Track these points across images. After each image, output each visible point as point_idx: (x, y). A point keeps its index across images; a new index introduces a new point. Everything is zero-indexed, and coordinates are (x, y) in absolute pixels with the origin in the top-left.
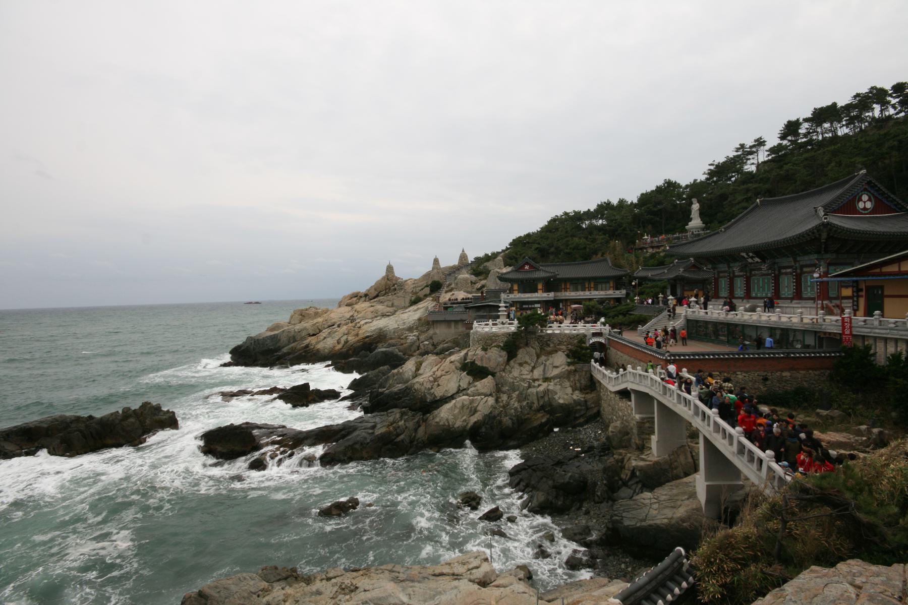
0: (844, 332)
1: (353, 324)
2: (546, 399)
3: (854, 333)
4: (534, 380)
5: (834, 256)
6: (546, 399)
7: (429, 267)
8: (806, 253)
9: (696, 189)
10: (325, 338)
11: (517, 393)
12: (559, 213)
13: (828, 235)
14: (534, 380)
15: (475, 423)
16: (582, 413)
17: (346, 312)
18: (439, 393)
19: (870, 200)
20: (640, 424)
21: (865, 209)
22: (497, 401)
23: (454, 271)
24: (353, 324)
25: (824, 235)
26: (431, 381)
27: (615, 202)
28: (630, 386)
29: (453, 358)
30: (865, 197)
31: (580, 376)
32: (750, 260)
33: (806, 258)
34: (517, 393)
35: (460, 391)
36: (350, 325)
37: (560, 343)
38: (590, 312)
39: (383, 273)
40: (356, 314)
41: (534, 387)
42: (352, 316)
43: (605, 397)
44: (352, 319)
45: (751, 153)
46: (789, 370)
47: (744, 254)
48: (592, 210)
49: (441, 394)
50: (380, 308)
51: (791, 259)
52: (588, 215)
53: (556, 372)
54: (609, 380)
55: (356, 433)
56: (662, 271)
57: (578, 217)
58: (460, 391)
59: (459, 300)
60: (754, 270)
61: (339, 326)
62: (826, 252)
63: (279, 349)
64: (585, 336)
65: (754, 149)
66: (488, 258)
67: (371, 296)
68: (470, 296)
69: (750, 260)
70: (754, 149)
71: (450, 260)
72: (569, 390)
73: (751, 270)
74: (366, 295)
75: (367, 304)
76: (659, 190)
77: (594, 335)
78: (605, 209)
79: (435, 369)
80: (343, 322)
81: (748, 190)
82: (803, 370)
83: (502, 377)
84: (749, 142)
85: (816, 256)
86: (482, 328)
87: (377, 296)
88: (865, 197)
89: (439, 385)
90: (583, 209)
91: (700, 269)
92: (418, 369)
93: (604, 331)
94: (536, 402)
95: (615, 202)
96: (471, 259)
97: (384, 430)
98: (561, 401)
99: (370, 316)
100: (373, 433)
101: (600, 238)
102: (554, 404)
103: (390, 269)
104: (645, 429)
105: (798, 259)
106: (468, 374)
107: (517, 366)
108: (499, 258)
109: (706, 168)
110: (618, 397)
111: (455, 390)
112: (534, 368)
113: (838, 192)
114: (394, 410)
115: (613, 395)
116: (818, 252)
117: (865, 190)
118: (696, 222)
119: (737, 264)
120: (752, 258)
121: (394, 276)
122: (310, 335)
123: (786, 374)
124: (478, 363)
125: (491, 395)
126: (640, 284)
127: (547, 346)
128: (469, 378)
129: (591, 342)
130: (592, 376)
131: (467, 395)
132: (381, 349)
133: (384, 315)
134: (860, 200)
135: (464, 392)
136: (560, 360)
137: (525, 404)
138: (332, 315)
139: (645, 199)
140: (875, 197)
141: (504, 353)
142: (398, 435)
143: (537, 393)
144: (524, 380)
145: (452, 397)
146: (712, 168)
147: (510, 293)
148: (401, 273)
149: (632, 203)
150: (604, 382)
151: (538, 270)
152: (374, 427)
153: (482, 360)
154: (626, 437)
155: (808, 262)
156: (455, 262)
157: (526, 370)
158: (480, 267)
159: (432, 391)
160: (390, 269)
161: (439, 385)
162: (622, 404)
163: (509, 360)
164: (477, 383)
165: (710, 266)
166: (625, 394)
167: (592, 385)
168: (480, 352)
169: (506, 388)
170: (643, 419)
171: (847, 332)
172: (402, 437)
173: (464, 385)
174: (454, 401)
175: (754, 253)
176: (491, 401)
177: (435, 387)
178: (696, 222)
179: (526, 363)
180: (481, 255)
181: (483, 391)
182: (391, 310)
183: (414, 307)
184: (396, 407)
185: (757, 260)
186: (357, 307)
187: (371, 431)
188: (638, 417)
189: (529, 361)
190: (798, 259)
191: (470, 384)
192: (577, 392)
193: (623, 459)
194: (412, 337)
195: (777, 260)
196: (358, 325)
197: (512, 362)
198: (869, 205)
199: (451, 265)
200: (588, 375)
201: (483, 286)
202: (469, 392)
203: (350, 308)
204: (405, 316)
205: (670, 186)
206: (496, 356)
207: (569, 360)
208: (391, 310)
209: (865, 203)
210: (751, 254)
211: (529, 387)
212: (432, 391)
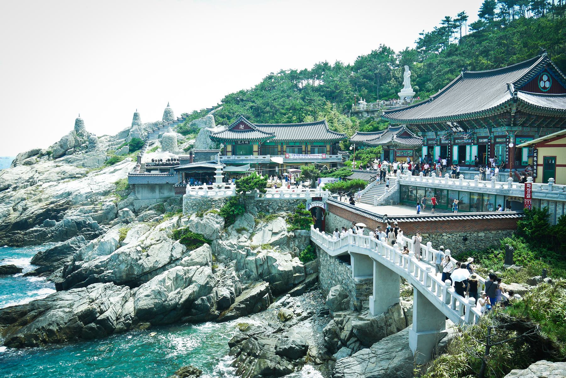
0: (526, 196)
1: (34, 187)
2: (266, 267)
3: (533, 197)
4: (254, 248)
5: (521, 128)
6: (266, 267)
7: (127, 124)
8: (499, 125)
9: (408, 57)
11: (235, 261)
12: (276, 71)
13: (517, 109)
14: (254, 248)
15: (190, 295)
16: (302, 279)
18: (148, 263)
19: (548, 80)
20: (359, 286)
21: (545, 88)
22: (214, 271)
23: (156, 128)
25: (514, 110)
26: (138, 252)
27: (332, 64)
28: (350, 250)
29: (163, 225)
30: (545, 78)
31: (299, 242)
32: (454, 129)
33: (499, 129)
34: (235, 261)
35: (173, 261)
37: (280, 209)
38: (311, 176)
40: (37, 175)
41: (253, 254)
42: (32, 178)
43: (323, 263)
45: (455, 27)
46: (484, 230)
47: (450, 124)
48: (309, 69)
49: (151, 265)
50: (69, 169)
51: (487, 130)
52: (305, 74)
54: (329, 243)
56: (377, 136)
57: (294, 76)
58: (173, 261)
59: (164, 161)
60: (458, 139)
61: (15, 189)
62: (515, 125)
64: (305, 201)
65: (458, 23)
66: (196, 115)
68: (177, 157)
69: (454, 129)
70: (458, 23)
71: (152, 116)
73: (455, 139)
74: (48, 153)
75: (51, 163)
76: (375, 55)
77: (314, 199)
78: (321, 70)
79: (143, 238)
81: (452, 62)
82: (494, 230)
83: (219, 245)
84: (454, 16)
85: (507, 128)
86: (195, 192)
87: (64, 154)
88: (545, 78)
89: (148, 256)
90: (299, 68)
91: (410, 137)
92: (122, 239)
93: (323, 196)
94: (254, 270)
95: (332, 64)
96: (177, 115)
99: (56, 177)
101: (317, 98)
102: (274, 272)
104: (364, 290)
105: (493, 130)
106: (181, 243)
107: (234, 233)
108: (210, 115)
109: (417, 37)
110: (337, 262)
111: (168, 260)
112: (252, 235)
113: (526, 71)
114: (95, 285)
115: (332, 260)
116: (509, 125)
117: (546, 71)
118: (407, 91)
119: (443, 132)
120: (456, 127)
123: (482, 234)
125: (207, 264)
126: (357, 149)
127: (267, 210)
129: (311, 207)
130: (311, 243)
131: (181, 265)
132: (72, 215)
133: (73, 177)
134: (541, 79)
135: (177, 263)
136: (280, 225)
137: (243, 272)
139: (361, 63)
140: (552, 78)
142: (102, 312)
143: (256, 260)
144: (242, 247)
145: (164, 268)
146: (422, 37)
147: (223, 155)
148: (92, 128)
149: (349, 66)
150: (324, 246)
151: (253, 130)
152: (71, 306)
153: (197, 227)
154: (345, 300)
155: (500, 134)
156: (159, 117)
157: (244, 237)
158: (188, 125)
159: (140, 262)
161: (148, 256)
162: (342, 268)
163: (226, 227)
164: (191, 252)
165: (420, 134)
166: (344, 258)
167: (311, 252)
168: (194, 218)
169: (222, 257)
170: (361, 281)
171: (528, 197)
173: (177, 254)
174: (166, 272)
175: (459, 122)
176: (208, 270)
177: (143, 257)
178: (407, 91)
179: (244, 229)
180: (190, 112)
181: (197, 260)
182: (83, 170)
183: (111, 168)
185: (460, 129)
187: (67, 310)
188: (357, 280)
189: (248, 228)
190: (493, 130)
191: (183, 253)
192: (297, 259)
193: (342, 321)
194: (110, 201)
195: (476, 131)
198: (548, 85)
199: (154, 121)
200: (307, 241)
201: (192, 146)
202: (183, 262)
203: (28, 168)
204: (99, 178)
205: (384, 53)
206: (213, 221)
207: (289, 226)
208: (83, 170)
209: (545, 83)
210: (455, 124)
211: (248, 255)
212: (140, 262)
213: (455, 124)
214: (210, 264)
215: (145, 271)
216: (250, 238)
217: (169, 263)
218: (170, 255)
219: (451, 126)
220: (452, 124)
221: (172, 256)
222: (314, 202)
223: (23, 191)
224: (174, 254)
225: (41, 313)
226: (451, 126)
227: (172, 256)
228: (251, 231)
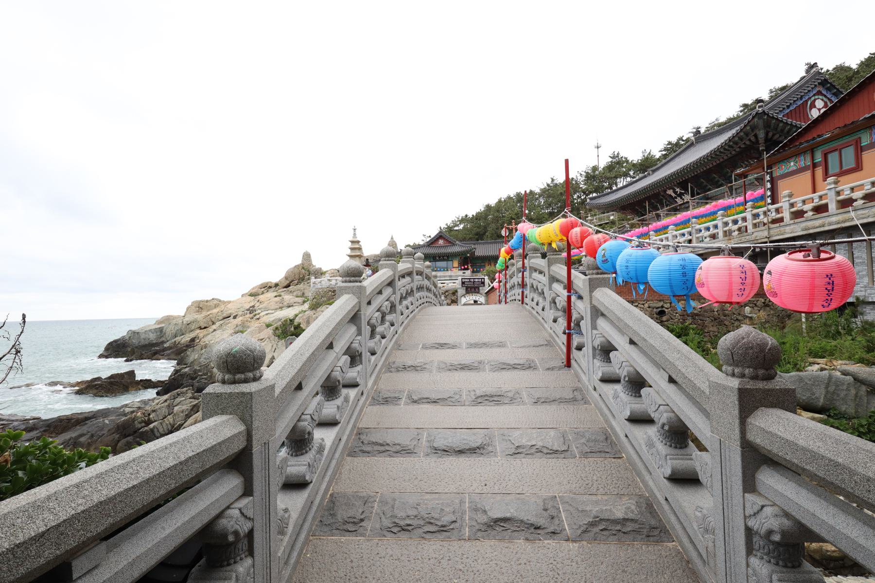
1: (252, 315)
10: (215, 330)
12: (504, 196)
17: (249, 302)
24: (252, 315)
36: (248, 315)
39: (298, 261)
40: (258, 304)
42: (253, 306)
44: (252, 310)
50: (288, 298)
61: (235, 317)
63: (163, 342)
67: (281, 285)
80: (240, 313)
103: (307, 256)
121: (311, 264)
122: (201, 328)
138: (229, 306)
148: (318, 262)
160: (307, 256)
182: (300, 300)
186: (261, 297)
196: (258, 316)
213: (678, 190)
219: (673, 195)
220: (675, 192)
223: (241, 318)
226: (673, 195)
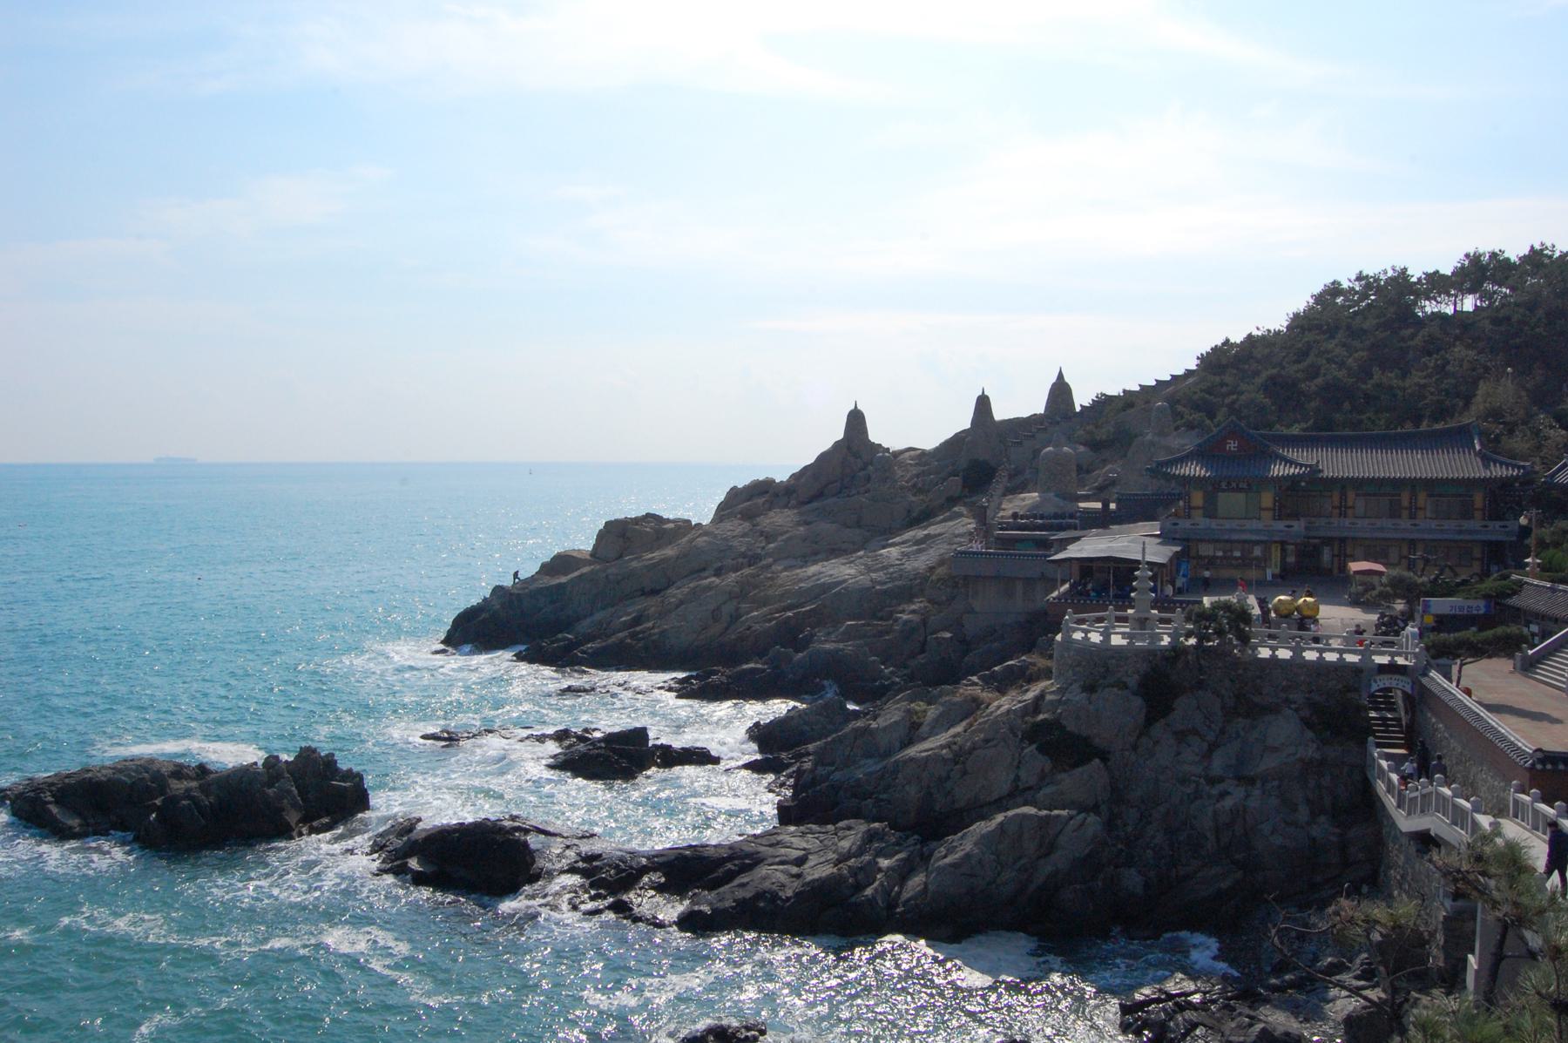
4: (1212, 781)
11: (1162, 809)
14: (1212, 781)
22: (1110, 825)
26: (945, 761)
34: (1162, 809)
53: (1269, 763)
55: (763, 870)
72: (1303, 813)
89: (965, 773)
97: (826, 871)
98: (1277, 840)
100: (798, 876)
106: (1041, 750)
111: (1005, 788)
112: (1213, 747)
124: (1071, 726)
125: (1095, 809)
128: (1044, 762)
141: (1138, 702)
142: (859, 887)
152: (800, 862)
159: (948, 785)
161: (965, 773)
163: (1150, 721)
172: (869, 891)
173: (1028, 777)
184: (857, 814)
187: (795, 870)
192: (1322, 819)
197: (1157, 729)
202: (1040, 795)
214: (1103, 808)
215: (957, 806)
216: (1208, 755)
217: (1011, 795)
218: (1012, 777)
221: (1017, 778)
222: (1386, 677)
224: (1023, 774)
225: (750, 868)
227: (1017, 778)
228: (1211, 737)
